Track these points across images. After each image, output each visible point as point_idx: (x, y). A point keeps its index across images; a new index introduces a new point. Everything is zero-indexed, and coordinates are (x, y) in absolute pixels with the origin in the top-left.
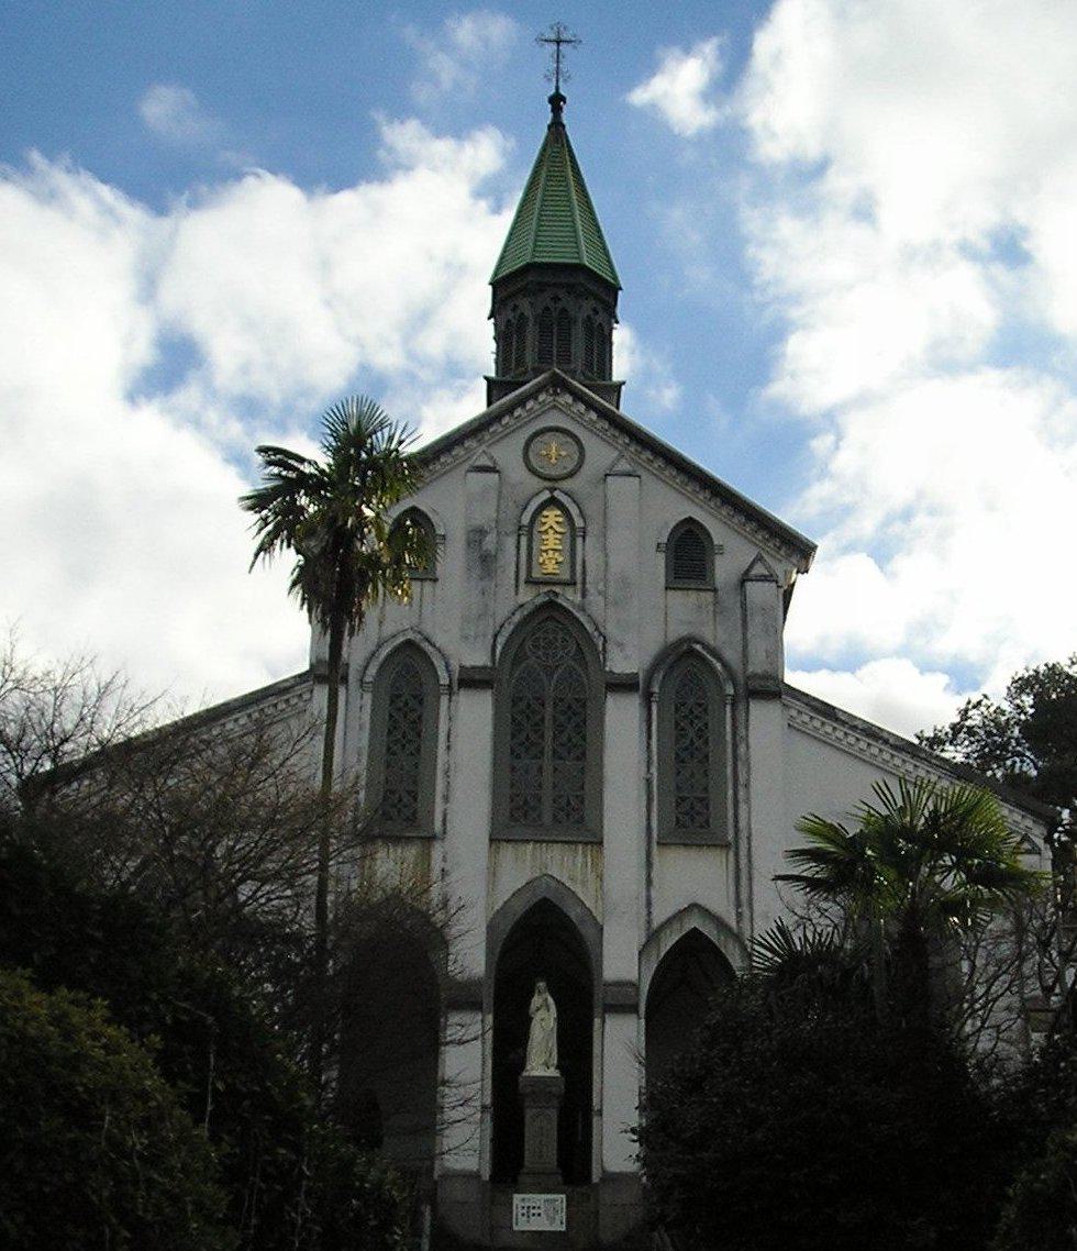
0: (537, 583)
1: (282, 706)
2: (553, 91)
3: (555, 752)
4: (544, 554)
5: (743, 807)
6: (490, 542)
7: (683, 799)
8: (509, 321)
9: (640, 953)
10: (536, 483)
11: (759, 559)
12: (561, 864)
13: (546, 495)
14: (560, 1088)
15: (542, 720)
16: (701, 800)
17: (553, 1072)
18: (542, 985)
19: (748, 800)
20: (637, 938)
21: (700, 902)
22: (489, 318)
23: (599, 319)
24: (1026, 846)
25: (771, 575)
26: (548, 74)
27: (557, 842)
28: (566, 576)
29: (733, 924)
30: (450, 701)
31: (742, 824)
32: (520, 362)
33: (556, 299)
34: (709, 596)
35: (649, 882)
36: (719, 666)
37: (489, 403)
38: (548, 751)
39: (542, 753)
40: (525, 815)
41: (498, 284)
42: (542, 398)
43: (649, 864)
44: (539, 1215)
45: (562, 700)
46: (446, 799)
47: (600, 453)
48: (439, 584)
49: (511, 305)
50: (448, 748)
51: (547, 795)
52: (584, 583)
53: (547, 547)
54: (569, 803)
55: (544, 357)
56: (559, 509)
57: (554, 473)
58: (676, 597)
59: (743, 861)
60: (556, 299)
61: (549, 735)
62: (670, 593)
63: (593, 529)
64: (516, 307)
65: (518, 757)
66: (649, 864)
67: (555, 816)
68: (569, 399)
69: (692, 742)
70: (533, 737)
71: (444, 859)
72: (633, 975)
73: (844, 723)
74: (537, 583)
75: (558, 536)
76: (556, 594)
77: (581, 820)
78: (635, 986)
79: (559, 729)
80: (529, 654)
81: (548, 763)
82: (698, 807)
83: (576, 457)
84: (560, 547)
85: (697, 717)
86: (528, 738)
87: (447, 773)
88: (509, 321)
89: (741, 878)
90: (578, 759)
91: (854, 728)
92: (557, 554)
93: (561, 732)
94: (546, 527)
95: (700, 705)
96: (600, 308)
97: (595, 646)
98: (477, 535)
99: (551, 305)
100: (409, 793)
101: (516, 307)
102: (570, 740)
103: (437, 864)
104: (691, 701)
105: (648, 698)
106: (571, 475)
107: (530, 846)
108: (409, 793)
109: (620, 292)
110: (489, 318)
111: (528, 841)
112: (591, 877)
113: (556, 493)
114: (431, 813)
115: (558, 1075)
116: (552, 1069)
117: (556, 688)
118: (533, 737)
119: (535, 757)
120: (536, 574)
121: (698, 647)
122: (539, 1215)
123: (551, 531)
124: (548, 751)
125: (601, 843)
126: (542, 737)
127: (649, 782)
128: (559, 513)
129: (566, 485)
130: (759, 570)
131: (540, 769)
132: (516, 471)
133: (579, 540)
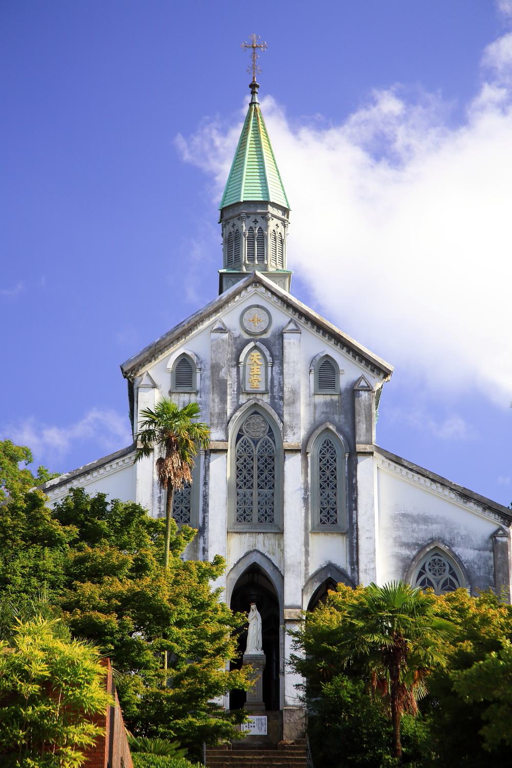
0: (248, 394)
1: (121, 463)
2: (250, 82)
3: (259, 485)
4: (252, 377)
5: (355, 512)
6: (222, 374)
7: (324, 509)
8: (230, 233)
9: (302, 590)
10: (246, 337)
11: (362, 378)
12: (263, 543)
13: (252, 345)
14: (263, 661)
15: (252, 468)
16: (333, 509)
17: (261, 652)
18: (253, 606)
19: (356, 509)
20: (301, 583)
21: (334, 562)
22: (219, 223)
23: (279, 230)
24: (501, 532)
25: (368, 386)
26: (248, 69)
27: (260, 533)
28: (263, 389)
29: (349, 573)
30: (205, 458)
31: (354, 521)
32: (238, 258)
33: (256, 222)
34: (336, 398)
35: (307, 553)
36: (341, 437)
37: (221, 292)
38: (255, 485)
39: (252, 485)
40: (245, 518)
41: (223, 210)
42: (249, 289)
43: (306, 544)
44: (254, 727)
45: (262, 457)
46: (205, 511)
47: (281, 318)
48: (199, 394)
49: (231, 224)
50: (206, 484)
51: (255, 508)
52: (272, 392)
53: (254, 373)
54: (266, 512)
55: (251, 257)
56: (260, 352)
57: (258, 330)
58: (320, 399)
59: (355, 541)
60: (256, 222)
61: (255, 476)
62: (316, 396)
63: (276, 362)
64: (234, 225)
65: (240, 488)
66: (306, 544)
67: (259, 519)
68: (263, 289)
69: (328, 479)
70: (248, 477)
71: (204, 543)
72: (299, 603)
73: (406, 467)
74: (248, 394)
75: (259, 367)
76: (258, 400)
77: (272, 521)
78: (300, 608)
79: (261, 472)
80: (245, 432)
81: (255, 491)
82: (332, 513)
83: (267, 321)
84: (259, 373)
85: (331, 465)
86: (245, 478)
87: (206, 497)
88: (230, 233)
89: (354, 550)
90: (270, 488)
91: (411, 470)
92: (258, 377)
93: (262, 474)
94: (254, 361)
95: (332, 458)
96: (279, 222)
97: (279, 429)
98: (216, 368)
99: (253, 225)
100: (186, 508)
101: (234, 225)
102: (266, 478)
103: (201, 545)
104: (328, 456)
105: (305, 454)
106: (265, 332)
107: (248, 535)
108: (186, 508)
109: (290, 211)
110: (219, 223)
111: (246, 533)
112: (277, 550)
113: (258, 343)
114: (197, 517)
115: (263, 654)
116: (259, 650)
117: (259, 451)
118: (248, 477)
119: (249, 488)
120: (248, 388)
121: (331, 427)
122: (254, 727)
123: (255, 364)
124: (255, 485)
125: (282, 533)
126: (252, 477)
127: (305, 500)
128: (259, 354)
129: (264, 336)
130: (363, 383)
131: (252, 494)
132: (238, 331)
133: (270, 369)
